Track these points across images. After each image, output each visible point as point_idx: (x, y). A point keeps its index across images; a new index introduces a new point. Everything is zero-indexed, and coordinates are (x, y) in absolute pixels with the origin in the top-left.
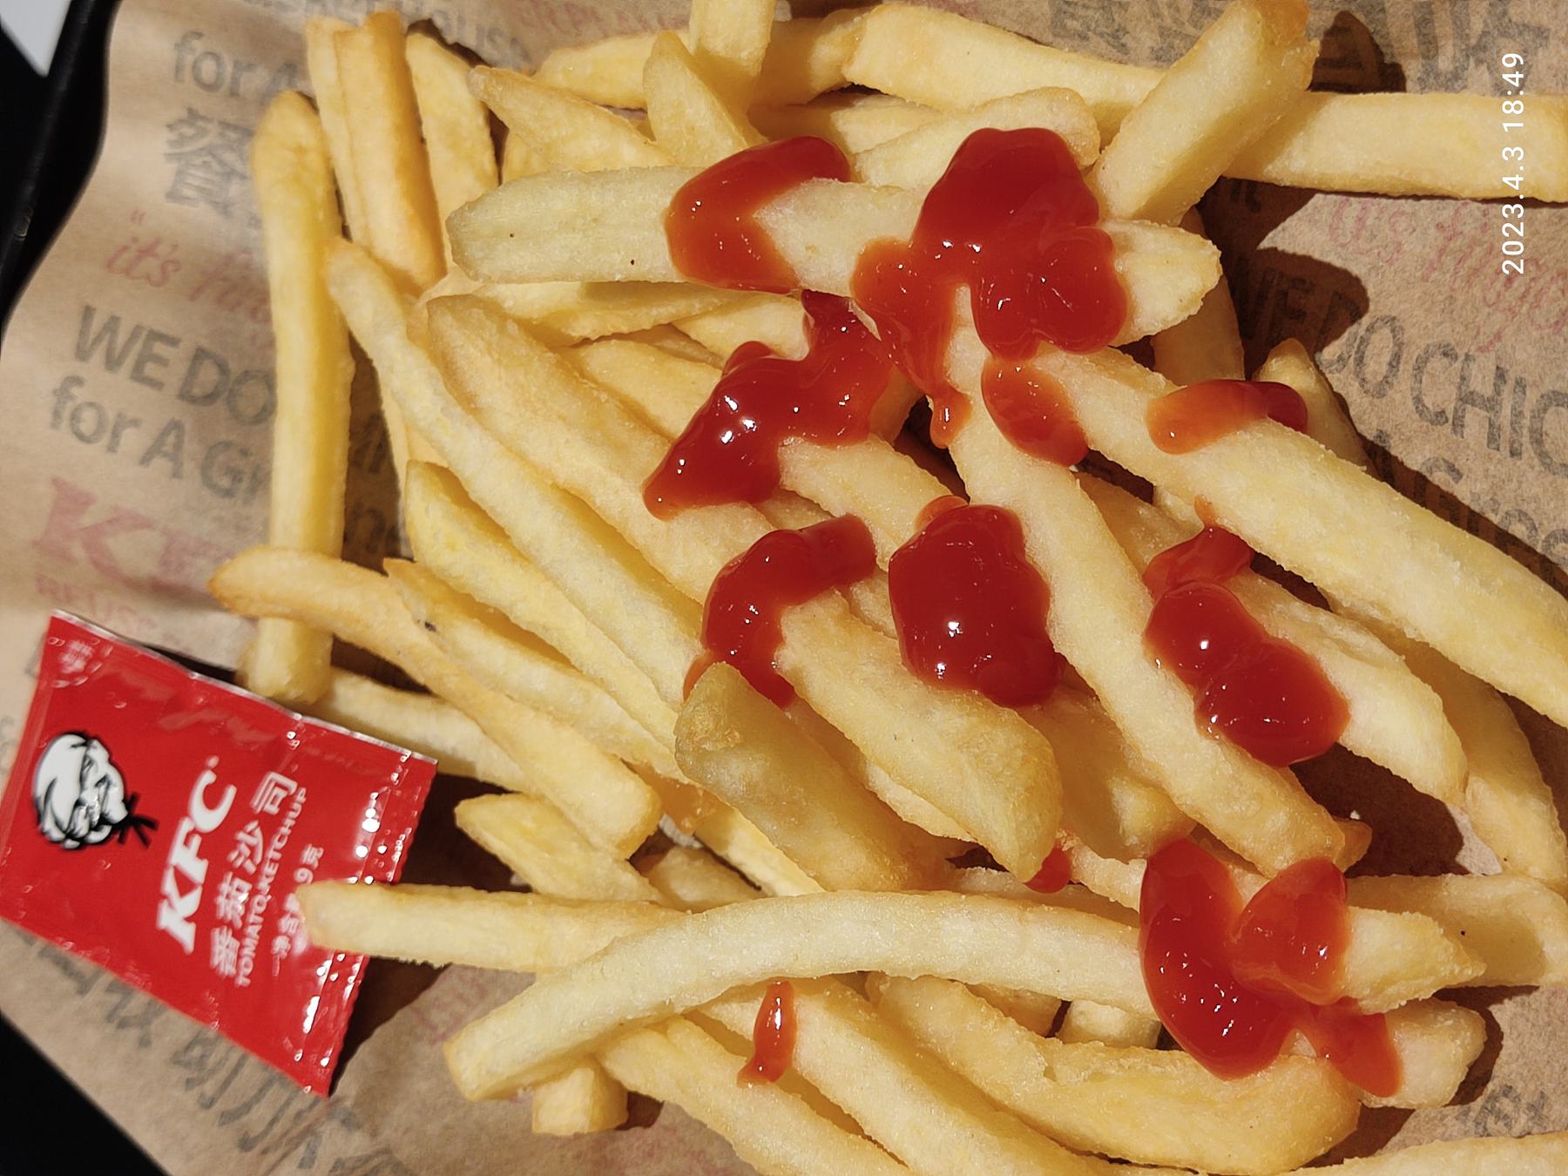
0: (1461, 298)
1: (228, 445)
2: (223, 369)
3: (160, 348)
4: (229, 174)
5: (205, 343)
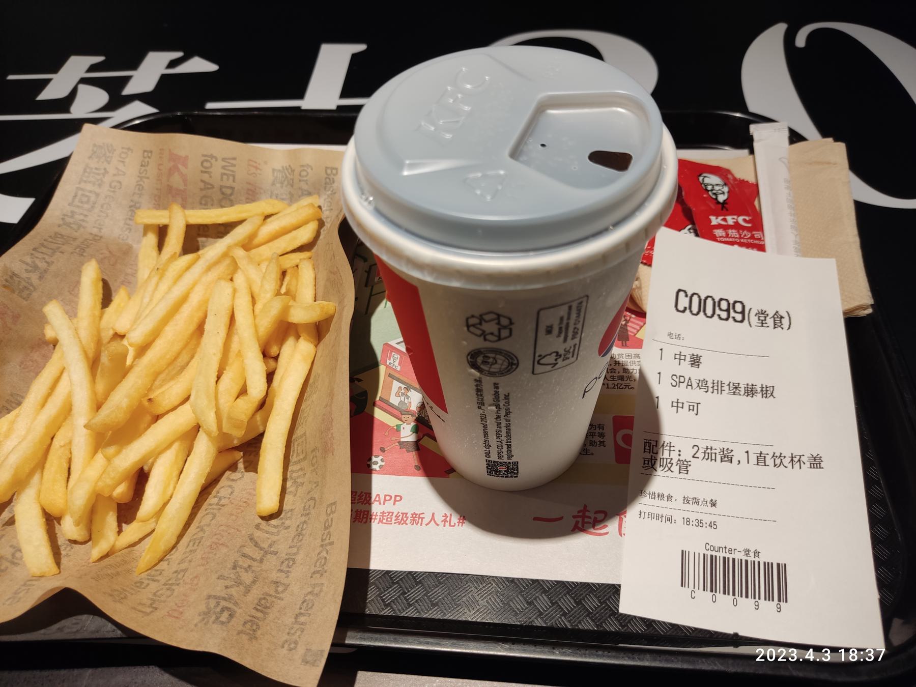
1: (213, 200)
2: (231, 195)
3: (231, 178)
4: (282, 183)
5: (236, 189)
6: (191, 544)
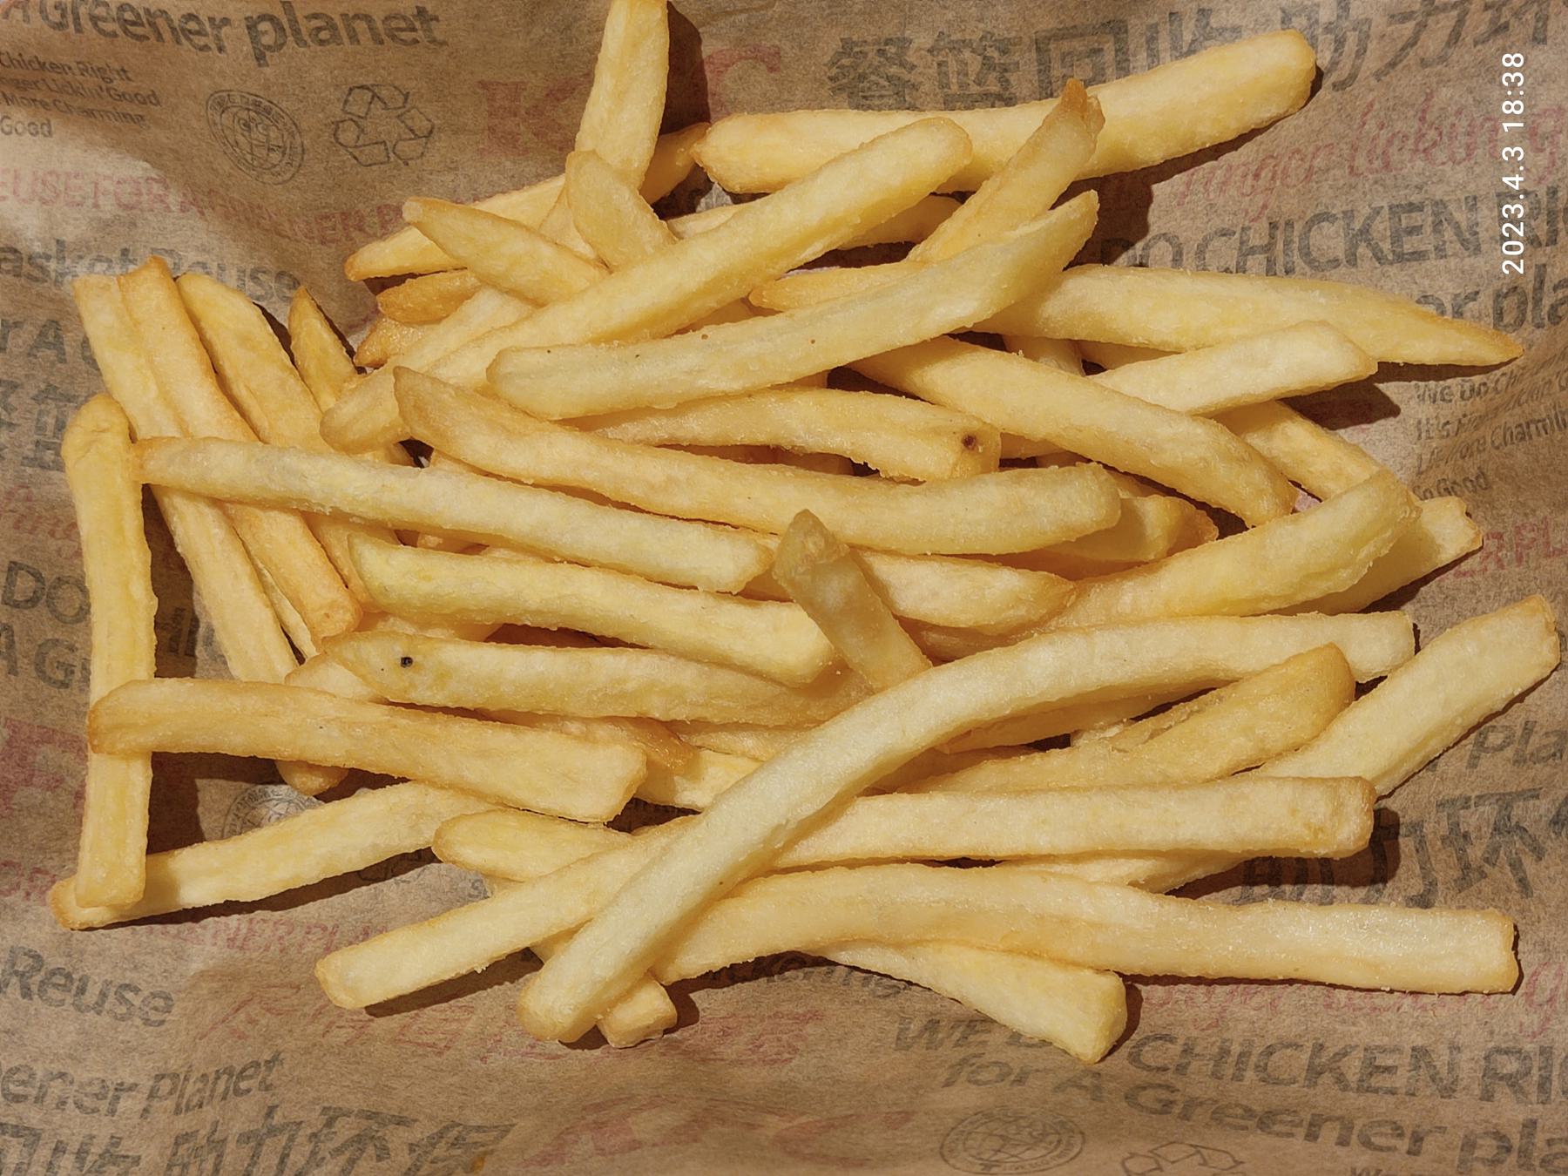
0: (1221, 201)
6: (1409, 245)
